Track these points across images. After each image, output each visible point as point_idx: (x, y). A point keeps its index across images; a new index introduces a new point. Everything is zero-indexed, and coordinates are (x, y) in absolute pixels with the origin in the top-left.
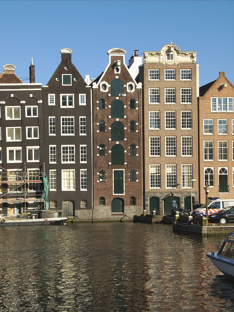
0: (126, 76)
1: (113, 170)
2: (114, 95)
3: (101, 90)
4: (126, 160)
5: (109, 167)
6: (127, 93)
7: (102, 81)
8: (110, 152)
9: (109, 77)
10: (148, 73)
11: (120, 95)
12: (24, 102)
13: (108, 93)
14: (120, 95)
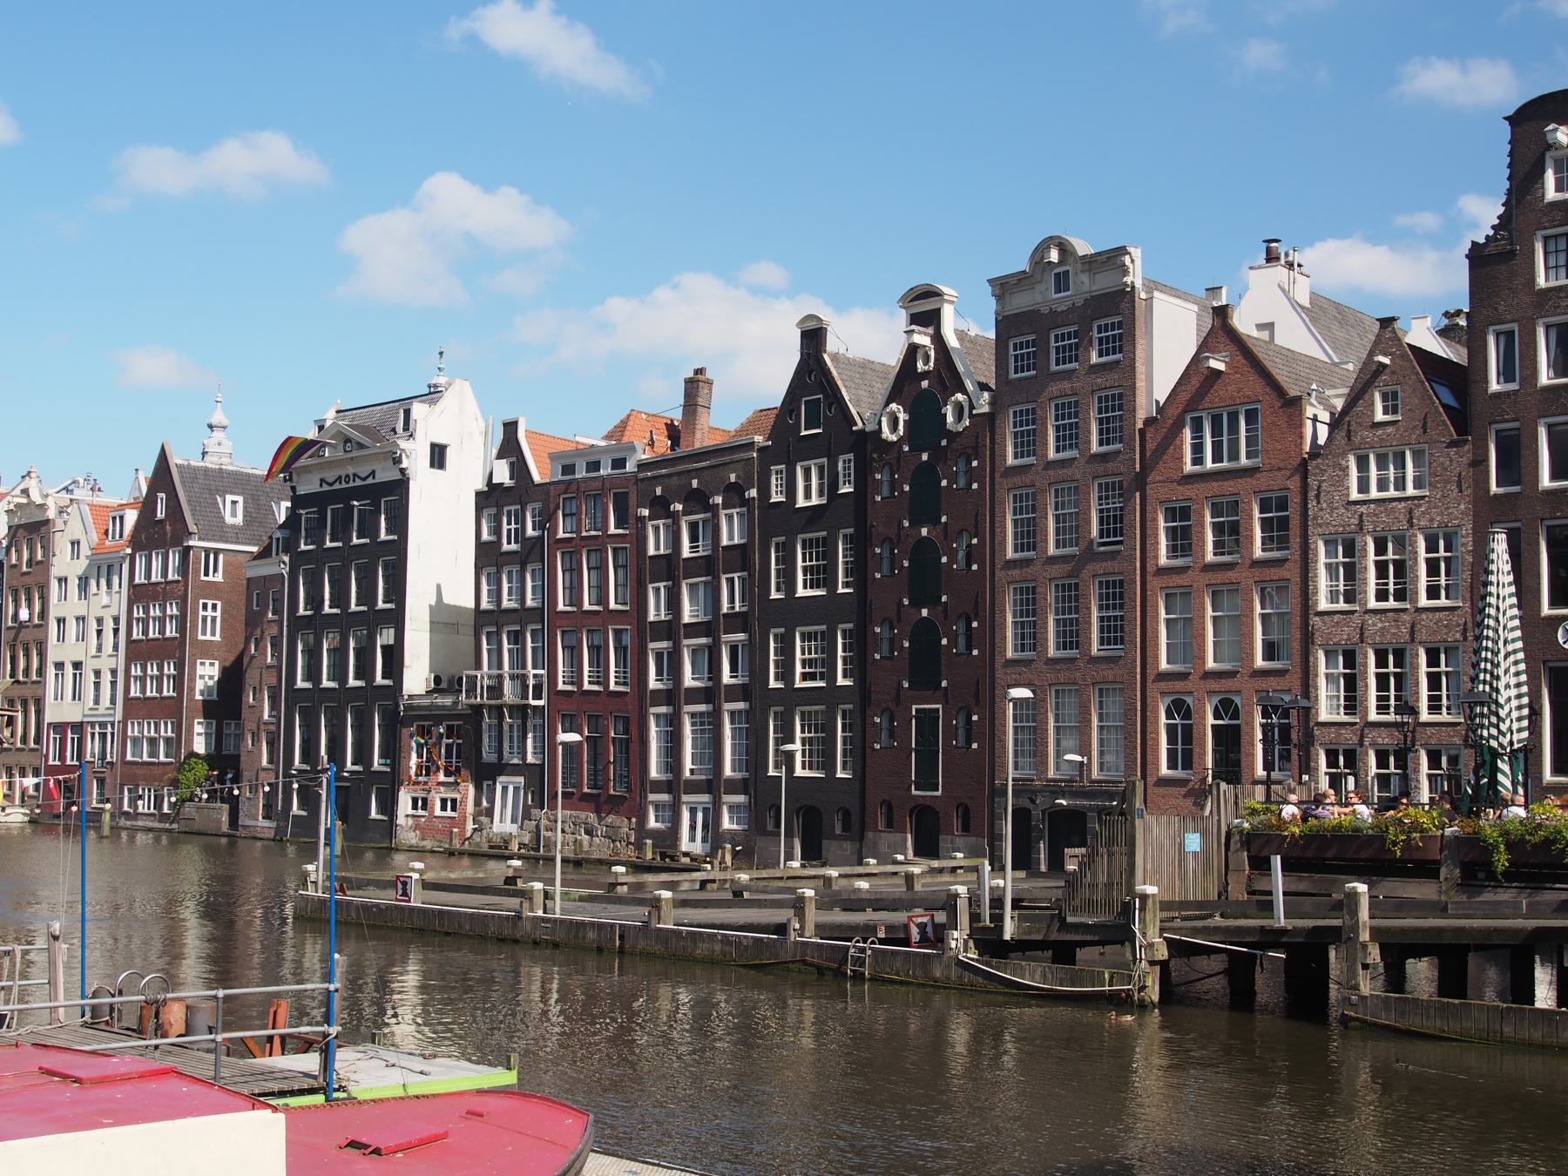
3: (886, 433)
10: (1007, 353)
13: (900, 439)
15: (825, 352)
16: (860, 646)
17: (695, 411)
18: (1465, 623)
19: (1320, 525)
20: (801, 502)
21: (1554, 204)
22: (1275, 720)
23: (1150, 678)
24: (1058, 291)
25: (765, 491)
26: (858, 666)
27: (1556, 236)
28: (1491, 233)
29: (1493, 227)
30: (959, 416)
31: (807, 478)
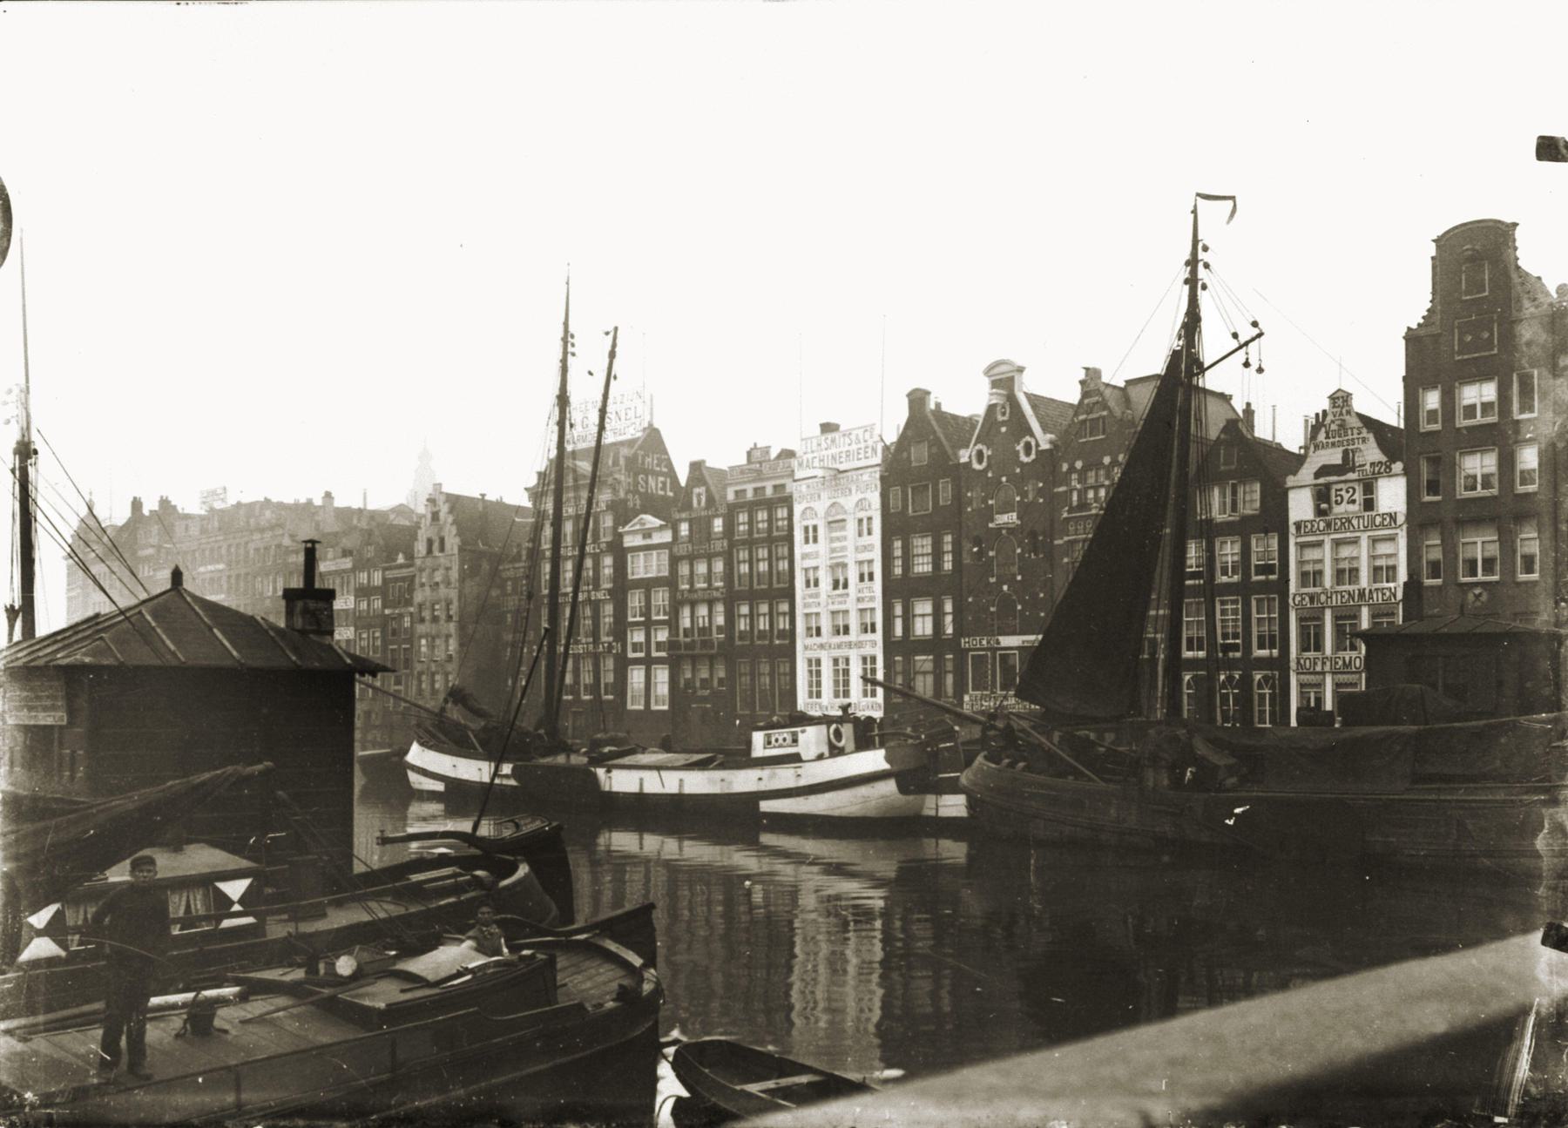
6: (1022, 465)
7: (975, 445)
13: (985, 471)
28: (1422, 321)
29: (1424, 317)
30: (1028, 453)
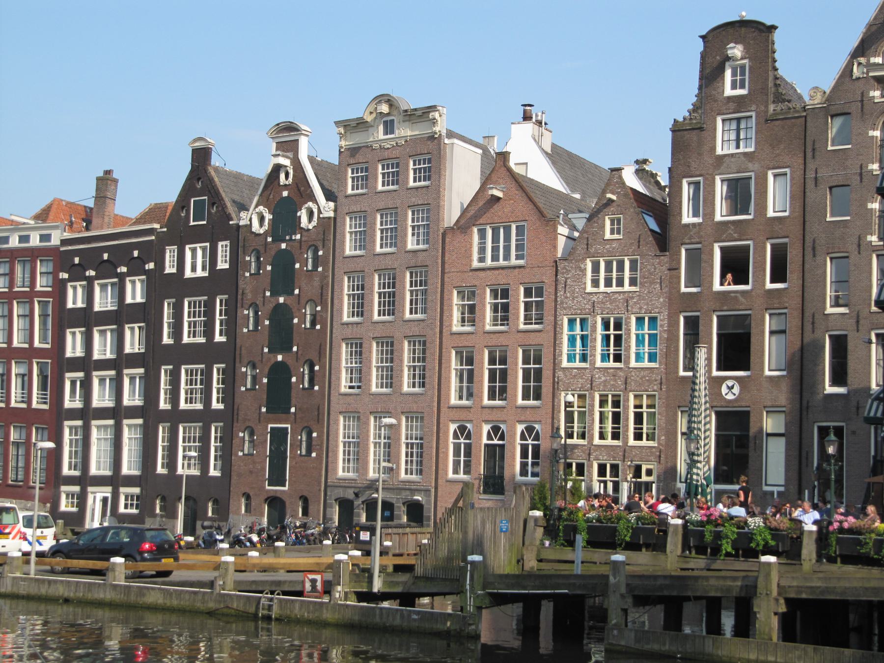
0: (302, 189)
1: (270, 426)
2: (278, 239)
4: (293, 401)
5: (262, 419)
7: (257, 206)
8: (265, 380)
9: (271, 197)
11: (288, 238)
12: (124, 269)
13: (266, 234)
14: (288, 238)
15: (210, 164)
16: (230, 380)
17: (104, 203)
18: (661, 379)
19: (565, 309)
20: (188, 274)
21: (729, 98)
22: (530, 442)
23: (444, 410)
24: (386, 133)
25: (161, 264)
26: (228, 395)
27: (730, 120)
31: (194, 256)
